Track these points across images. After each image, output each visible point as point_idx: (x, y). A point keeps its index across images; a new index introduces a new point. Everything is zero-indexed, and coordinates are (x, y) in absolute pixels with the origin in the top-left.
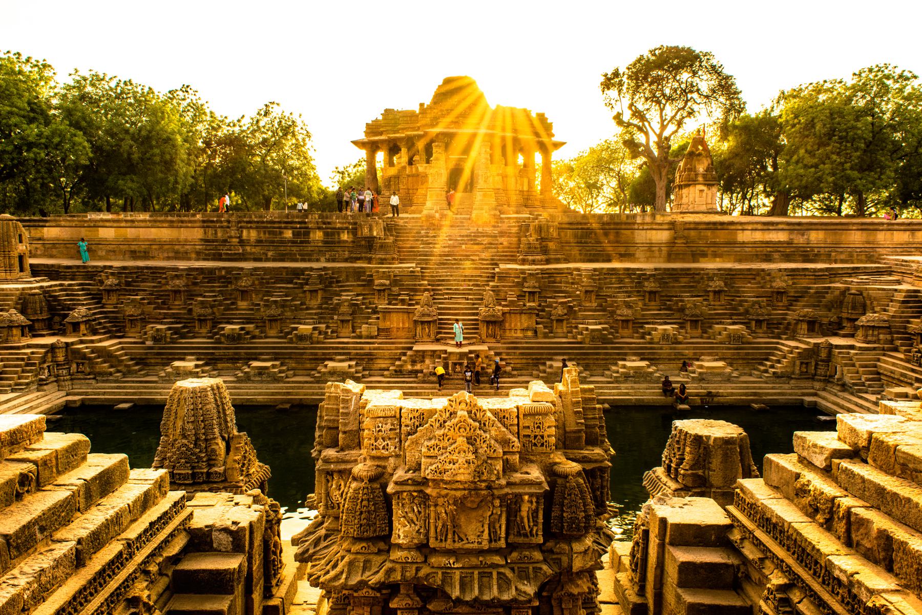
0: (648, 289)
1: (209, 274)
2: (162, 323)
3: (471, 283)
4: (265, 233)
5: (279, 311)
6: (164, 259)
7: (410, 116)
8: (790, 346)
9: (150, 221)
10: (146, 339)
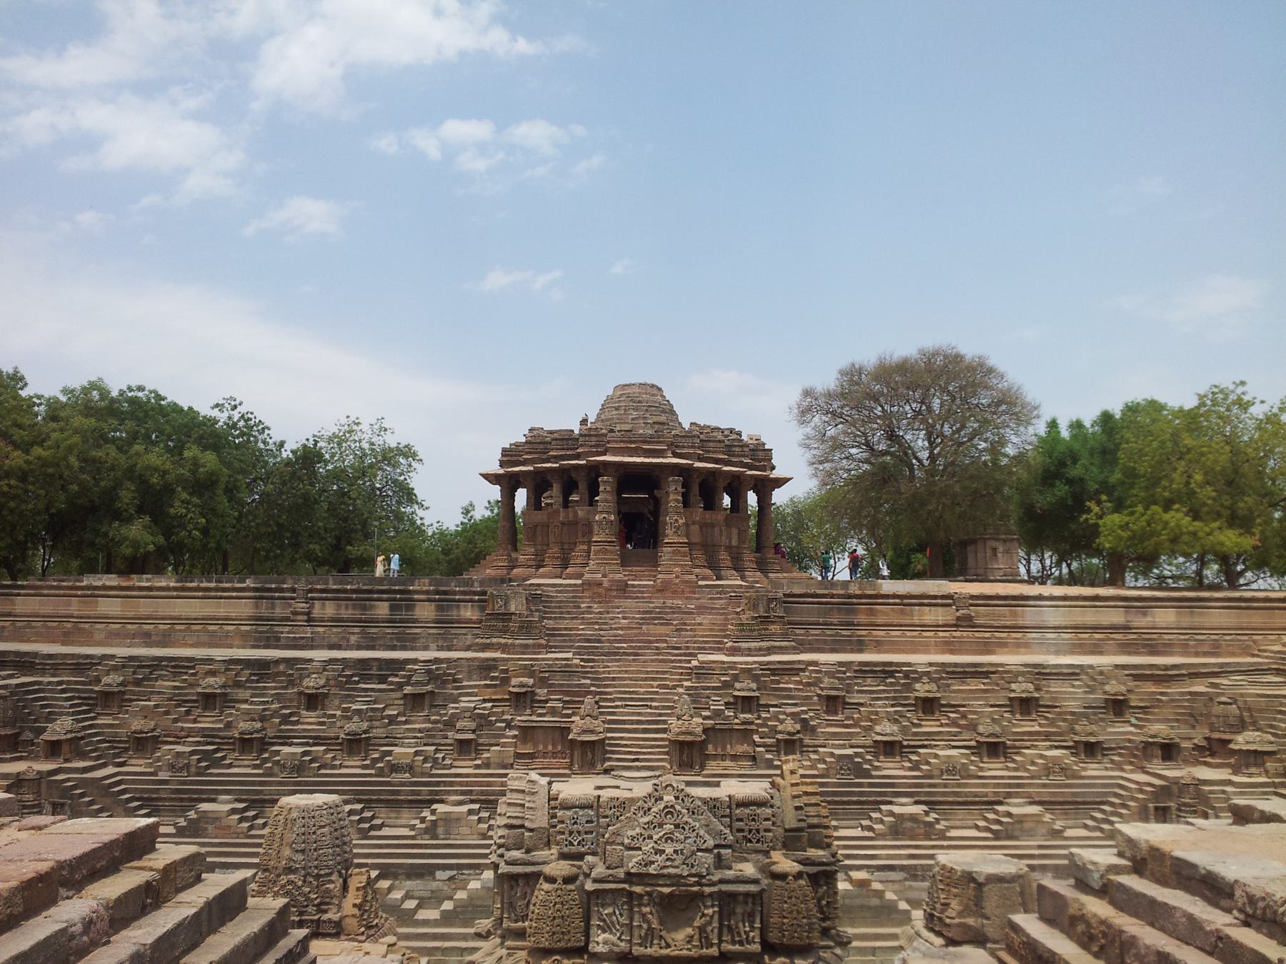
0: (922, 695)
1: (261, 667)
2: (184, 744)
4: (347, 608)
5: (365, 725)
6: (192, 646)
7: (565, 439)
8: (1137, 783)
9: (175, 589)
10: (159, 769)
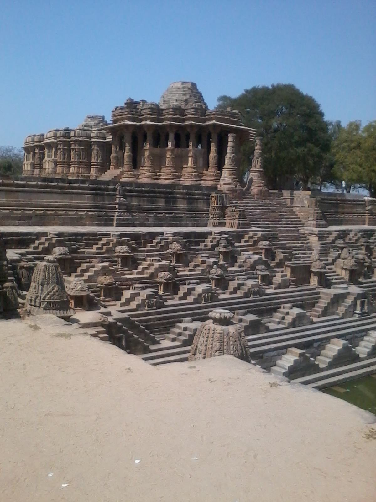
3: (300, 242)
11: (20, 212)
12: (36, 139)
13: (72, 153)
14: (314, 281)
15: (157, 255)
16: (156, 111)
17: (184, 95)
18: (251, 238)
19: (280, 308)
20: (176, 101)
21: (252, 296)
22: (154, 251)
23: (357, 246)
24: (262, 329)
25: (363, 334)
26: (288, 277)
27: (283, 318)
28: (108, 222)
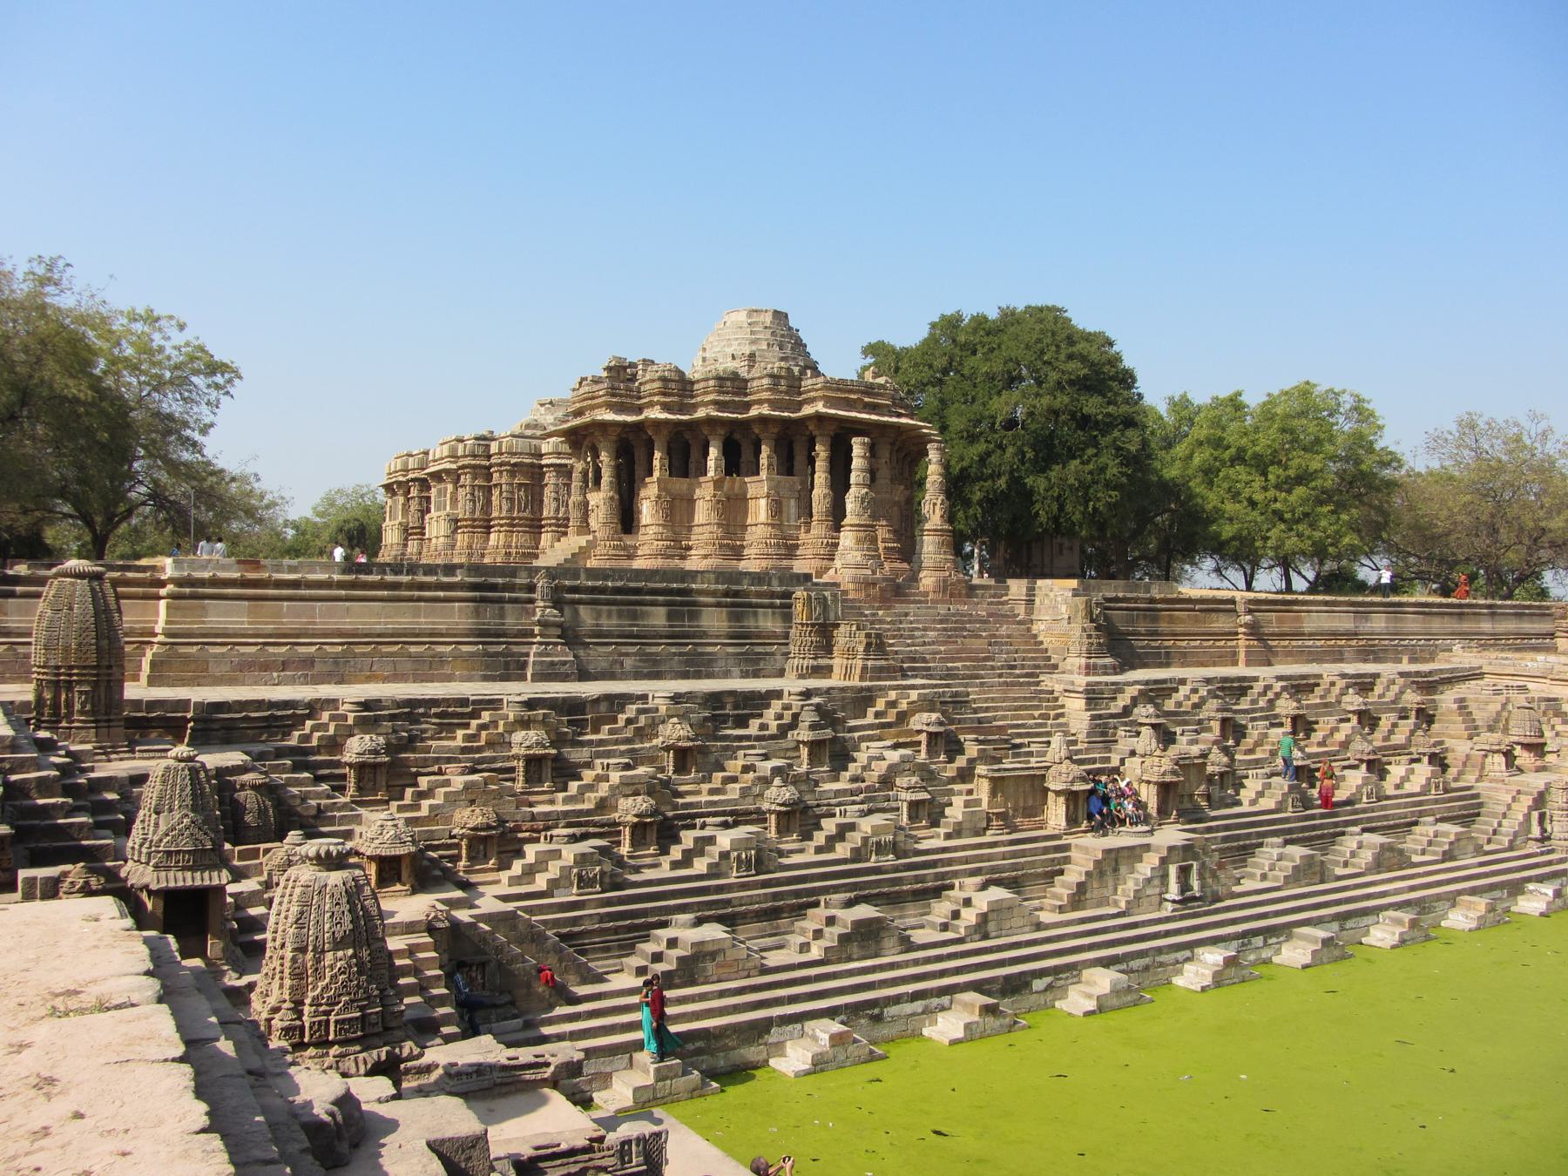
3: (1036, 713)
6: (385, 680)
11: (284, 649)
12: (412, 463)
13: (496, 492)
14: (1056, 814)
15: (622, 754)
16: (679, 387)
17: (753, 342)
18: (892, 704)
19: (951, 887)
20: (733, 357)
21: (874, 858)
22: (617, 742)
23: (1200, 722)
24: (890, 943)
25: (1180, 955)
26: (985, 805)
27: (956, 915)
28: (512, 669)
